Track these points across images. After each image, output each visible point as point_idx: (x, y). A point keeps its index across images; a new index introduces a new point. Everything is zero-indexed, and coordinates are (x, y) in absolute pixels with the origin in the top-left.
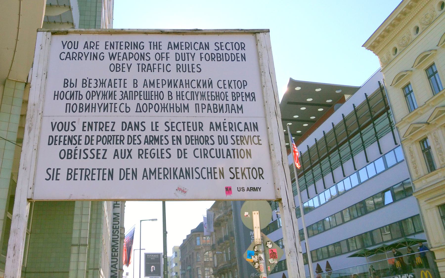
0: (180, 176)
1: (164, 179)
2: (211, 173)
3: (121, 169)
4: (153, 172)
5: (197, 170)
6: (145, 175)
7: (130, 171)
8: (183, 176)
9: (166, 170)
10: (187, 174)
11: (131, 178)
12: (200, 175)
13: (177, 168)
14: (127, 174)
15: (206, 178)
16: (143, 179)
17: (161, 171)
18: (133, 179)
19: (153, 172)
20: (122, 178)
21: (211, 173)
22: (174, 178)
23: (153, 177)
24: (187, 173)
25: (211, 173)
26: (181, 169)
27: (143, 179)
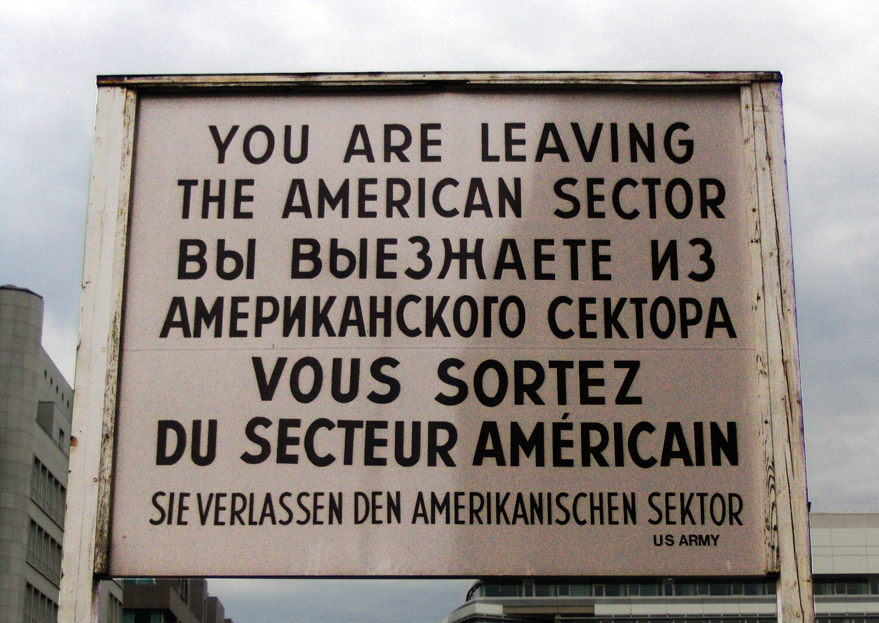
0: (516, 516)
1: (471, 522)
2: (602, 508)
3: (357, 494)
4: (441, 500)
5: (563, 500)
6: (420, 511)
7: (382, 500)
8: (524, 516)
9: (477, 499)
10: (534, 510)
11: (385, 520)
12: (572, 515)
13: (508, 495)
14: (375, 507)
15: (584, 522)
16: (414, 522)
17: (464, 501)
18: (389, 521)
19: (441, 500)
20: (360, 519)
21: (602, 508)
22: (498, 522)
23: (440, 518)
24: (537, 508)
25: (600, 508)
26: (520, 497)
27: (414, 522)
